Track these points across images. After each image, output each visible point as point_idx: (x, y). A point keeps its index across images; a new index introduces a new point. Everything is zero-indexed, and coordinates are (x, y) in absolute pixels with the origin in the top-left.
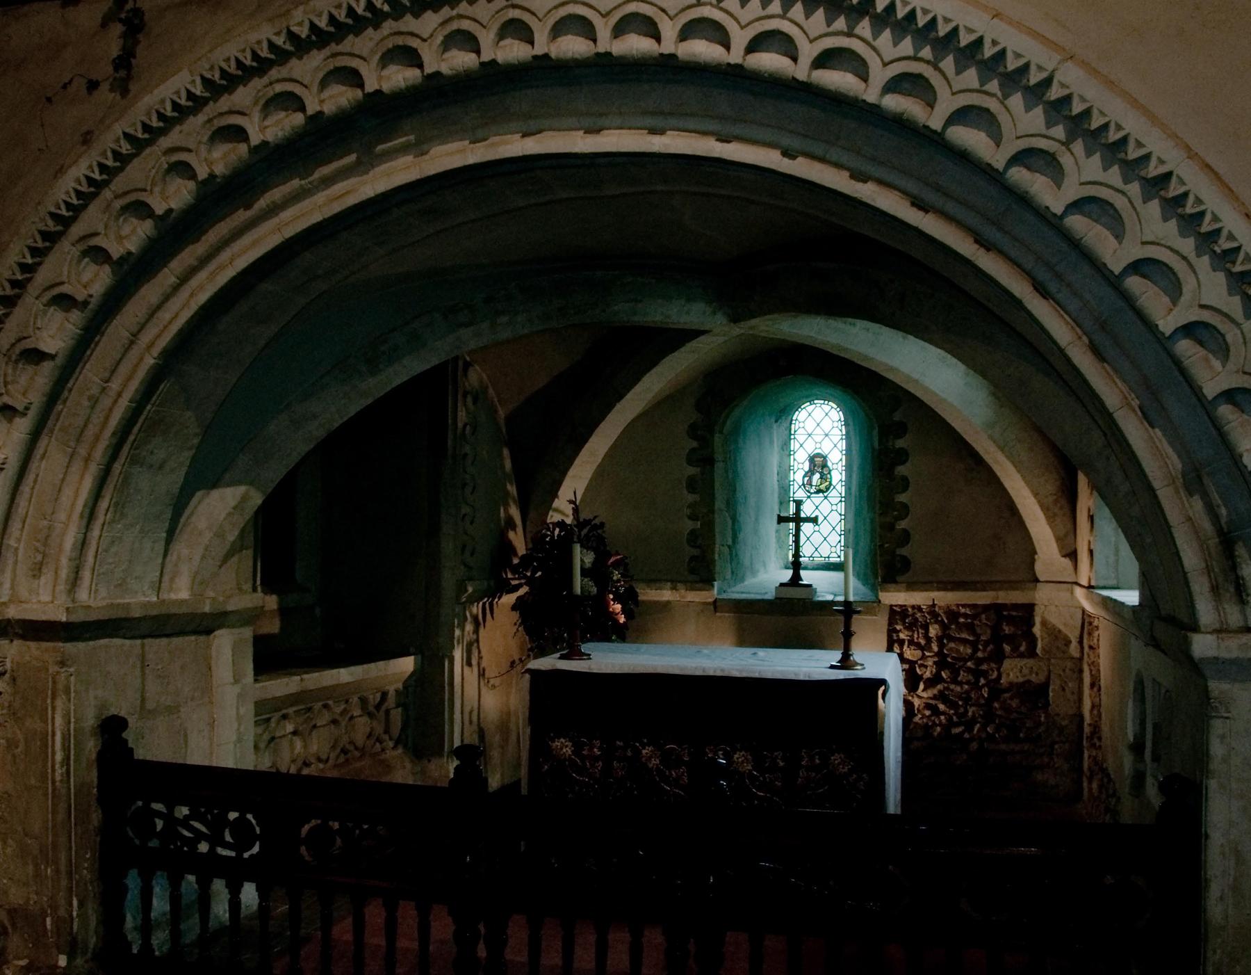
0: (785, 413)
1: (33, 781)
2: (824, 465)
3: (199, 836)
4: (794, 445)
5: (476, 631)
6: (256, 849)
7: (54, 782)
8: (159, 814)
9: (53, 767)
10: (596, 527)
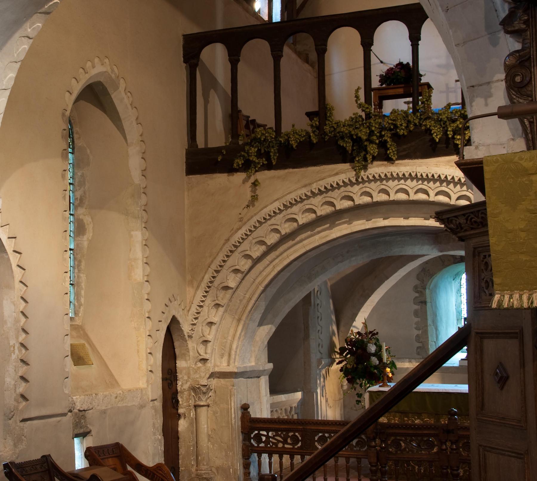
1: (224, 425)
3: (279, 441)
5: (324, 381)
6: (300, 444)
8: (264, 435)
9: (231, 420)
10: (374, 334)
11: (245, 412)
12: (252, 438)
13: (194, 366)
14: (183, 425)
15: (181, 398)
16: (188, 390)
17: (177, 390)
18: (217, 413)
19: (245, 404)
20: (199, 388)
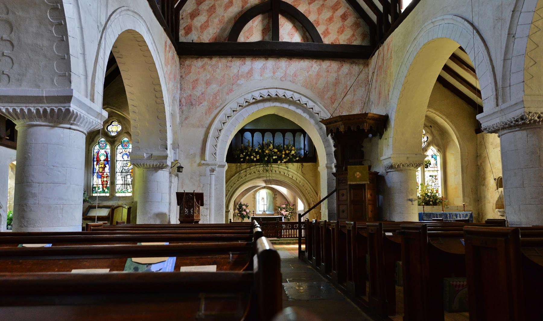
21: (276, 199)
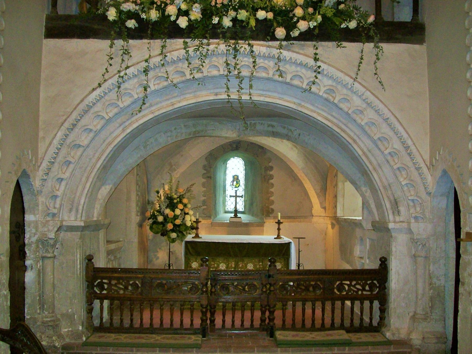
0: (225, 162)
2: (238, 179)
4: (227, 172)
7: (77, 274)
9: (77, 270)
11: (89, 262)
12: (96, 286)
13: (42, 220)
14: (30, 277)
15: (29, 250)
16: (35, 243)
17: (24, 243)
18: (63, 264)
19: (90, 255)
20: (46, 240)
21: (271, 181)
